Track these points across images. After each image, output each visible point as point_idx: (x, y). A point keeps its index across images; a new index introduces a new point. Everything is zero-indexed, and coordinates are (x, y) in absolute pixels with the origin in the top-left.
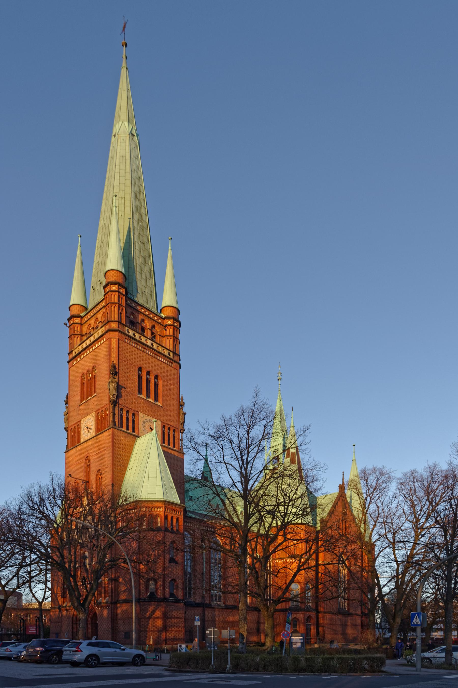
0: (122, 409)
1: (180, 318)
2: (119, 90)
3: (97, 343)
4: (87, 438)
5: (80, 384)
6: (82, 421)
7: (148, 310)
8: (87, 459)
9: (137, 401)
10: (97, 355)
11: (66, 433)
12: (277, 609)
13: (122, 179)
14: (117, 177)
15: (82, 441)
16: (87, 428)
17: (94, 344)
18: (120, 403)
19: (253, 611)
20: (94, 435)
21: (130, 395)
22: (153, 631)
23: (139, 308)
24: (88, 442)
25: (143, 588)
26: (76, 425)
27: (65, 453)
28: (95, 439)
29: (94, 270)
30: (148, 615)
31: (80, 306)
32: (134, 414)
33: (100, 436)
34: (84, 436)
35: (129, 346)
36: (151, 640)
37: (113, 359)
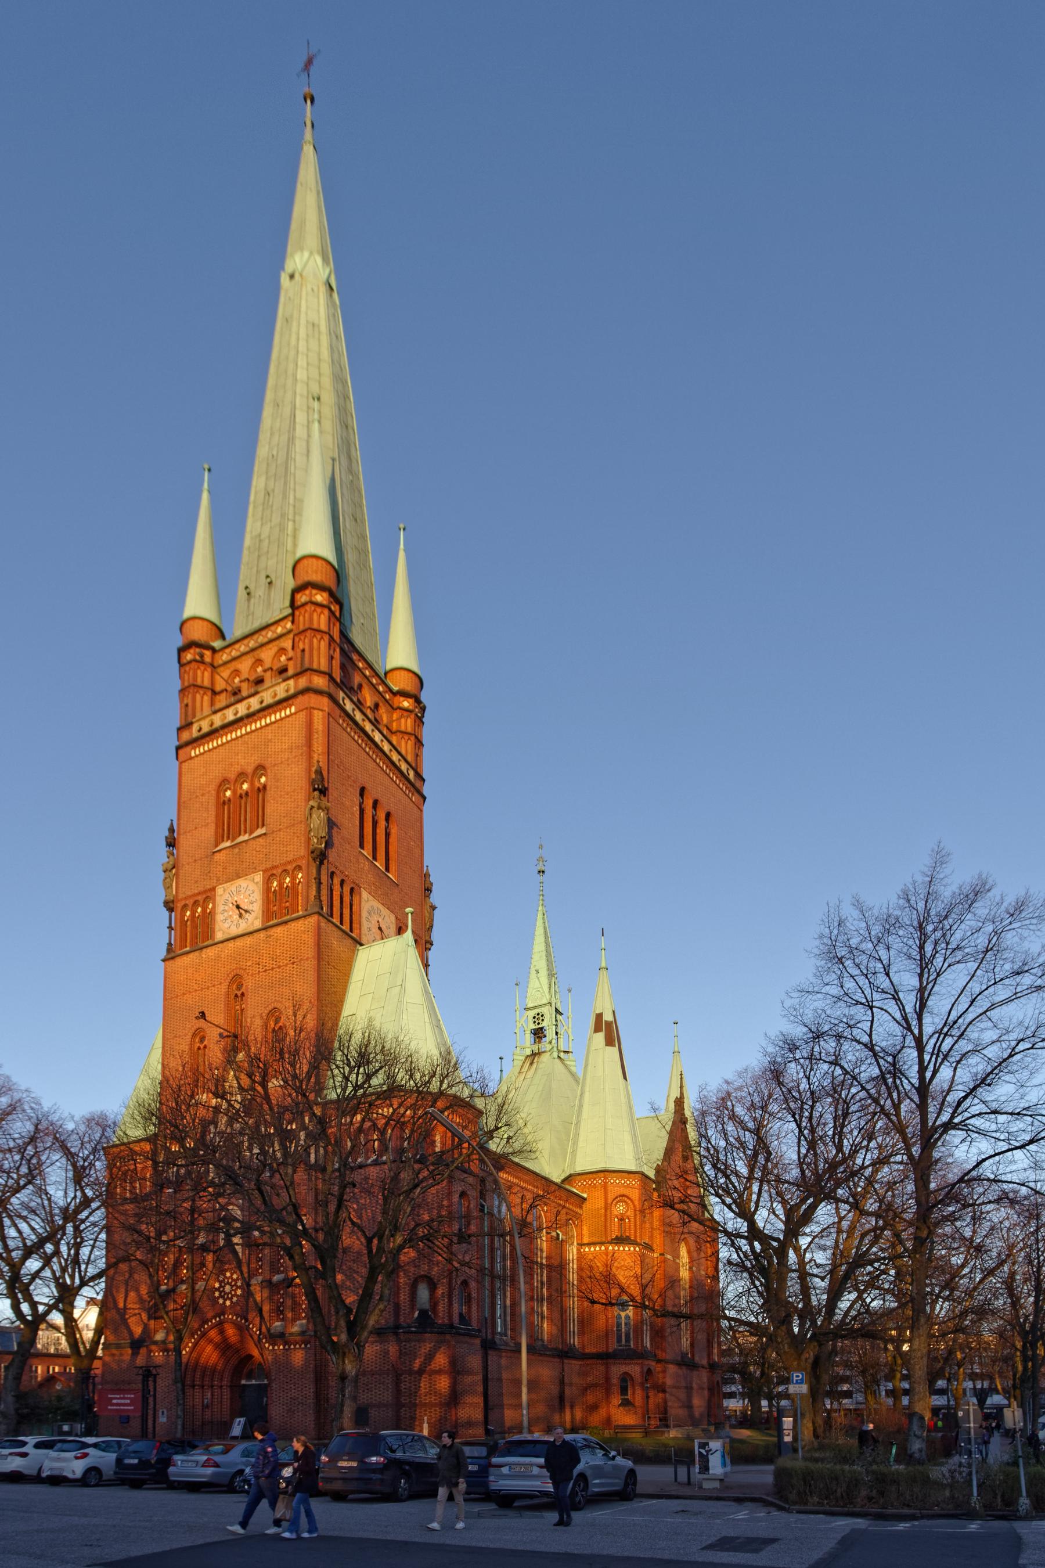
0: (333, 873)
1: (424, 697)
2: (299, 186)
3: (270, 715)
4: (234, 931)
5: (213, 800)
6: (219, 890)
7: (370, 666)
8: (237, 980)
9: (358, 862)
10: (270, 741)
11: (167, 913)
12: (589, 1354)
13: (314, 373)
14: (302, 362)
15: (219, 936)
16: (238, 907)
17: (260, 715)
18: (330, 859)
19: (553, 1356)
20: (258, 924)
21: (347, 846)
22: (431, 1405)
23: (355, 657)
24: (238, 940)
25: (404, 1297)
26: (200, 898)
27: (164, 960)
28: (262, 935)
29: (245, 552)
30: (417, 1364)
31: (210, 626)
32: (352, 890)
33: (279, 930)
34: (226, 925)
35: (345, 735)
36: (426, 1426)
37: (316, 757)
